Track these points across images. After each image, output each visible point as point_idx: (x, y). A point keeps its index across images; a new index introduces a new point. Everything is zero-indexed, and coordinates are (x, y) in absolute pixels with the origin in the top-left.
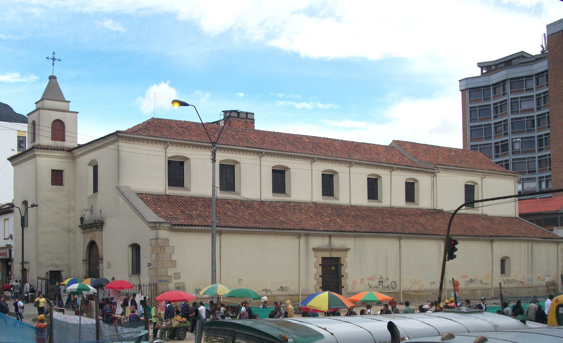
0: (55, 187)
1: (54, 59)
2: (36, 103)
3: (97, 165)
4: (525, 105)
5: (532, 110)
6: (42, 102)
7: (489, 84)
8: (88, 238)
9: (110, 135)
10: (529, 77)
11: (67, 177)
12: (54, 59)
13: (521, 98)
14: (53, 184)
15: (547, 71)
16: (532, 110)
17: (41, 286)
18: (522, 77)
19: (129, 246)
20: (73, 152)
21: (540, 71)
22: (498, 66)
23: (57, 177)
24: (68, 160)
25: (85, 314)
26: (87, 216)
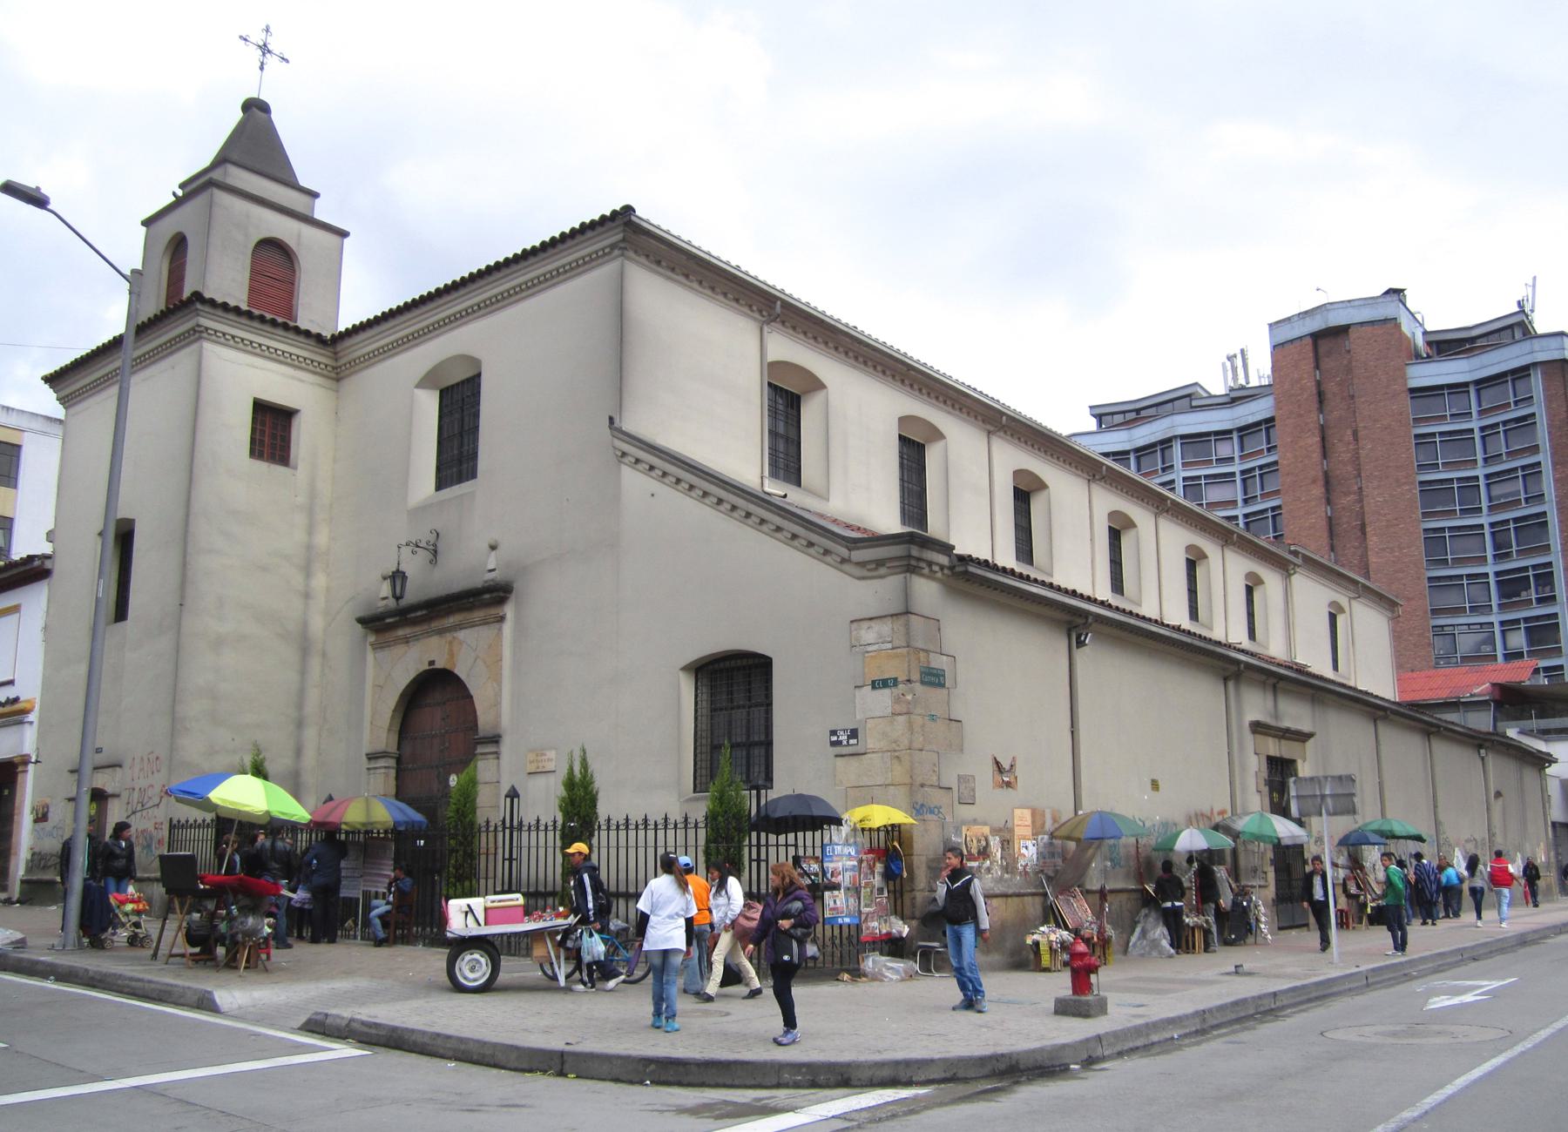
0: (262, 467)
1: (265, 49)
2: (147, 223)
3: (479, 375)
4: (1214, 494)
5: (1233, 503)
6: (199, 202)
7: (1127, 447)
8: (407, 661)
9: (585, 228)
10: (1224, 435)
11: (306, 436)
12: (265, 49)
13: (1206, 477)
14: (252, 454)
15: (1272, 419)
16: (1233, 503)
17: (650, 778)
18: (1208, 434)
19: (685, 669)
20: (337, 352)
21: (1251, 420)
22: (1143, 413)
23: (272, 429)
24: (318, 379)
25: (846, 976)
26: (413, 566)
